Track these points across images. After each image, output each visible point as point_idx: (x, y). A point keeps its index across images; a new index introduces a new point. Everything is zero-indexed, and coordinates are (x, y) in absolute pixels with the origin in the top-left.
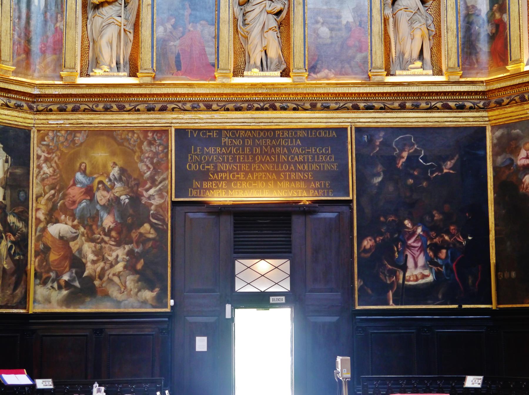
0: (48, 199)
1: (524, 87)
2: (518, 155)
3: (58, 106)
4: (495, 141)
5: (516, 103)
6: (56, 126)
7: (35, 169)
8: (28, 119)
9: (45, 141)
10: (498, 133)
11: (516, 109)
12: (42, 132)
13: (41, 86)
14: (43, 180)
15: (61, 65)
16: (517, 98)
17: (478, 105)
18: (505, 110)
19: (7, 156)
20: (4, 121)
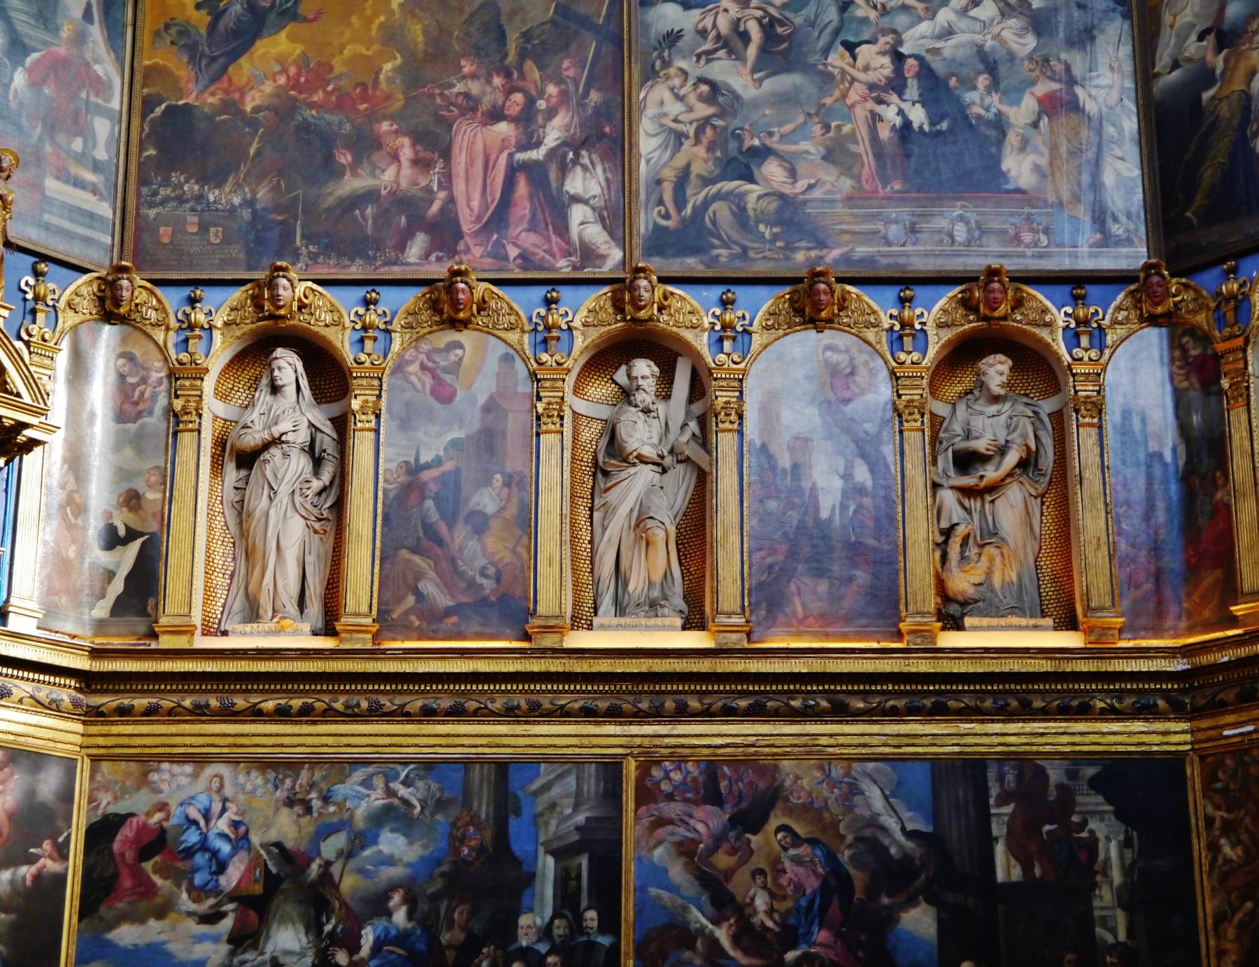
0: (1242, 926)
3: (1237, 690)
6: (1238, 739)
7: (1203, 854)
8: (1176, 733)
9: (1218, 780)
12: (1210, 759)
13: (1187, 651)
14: (1224, 878)
15: (1235, 589)
19: (1126, 832)
20: (1113, 749)
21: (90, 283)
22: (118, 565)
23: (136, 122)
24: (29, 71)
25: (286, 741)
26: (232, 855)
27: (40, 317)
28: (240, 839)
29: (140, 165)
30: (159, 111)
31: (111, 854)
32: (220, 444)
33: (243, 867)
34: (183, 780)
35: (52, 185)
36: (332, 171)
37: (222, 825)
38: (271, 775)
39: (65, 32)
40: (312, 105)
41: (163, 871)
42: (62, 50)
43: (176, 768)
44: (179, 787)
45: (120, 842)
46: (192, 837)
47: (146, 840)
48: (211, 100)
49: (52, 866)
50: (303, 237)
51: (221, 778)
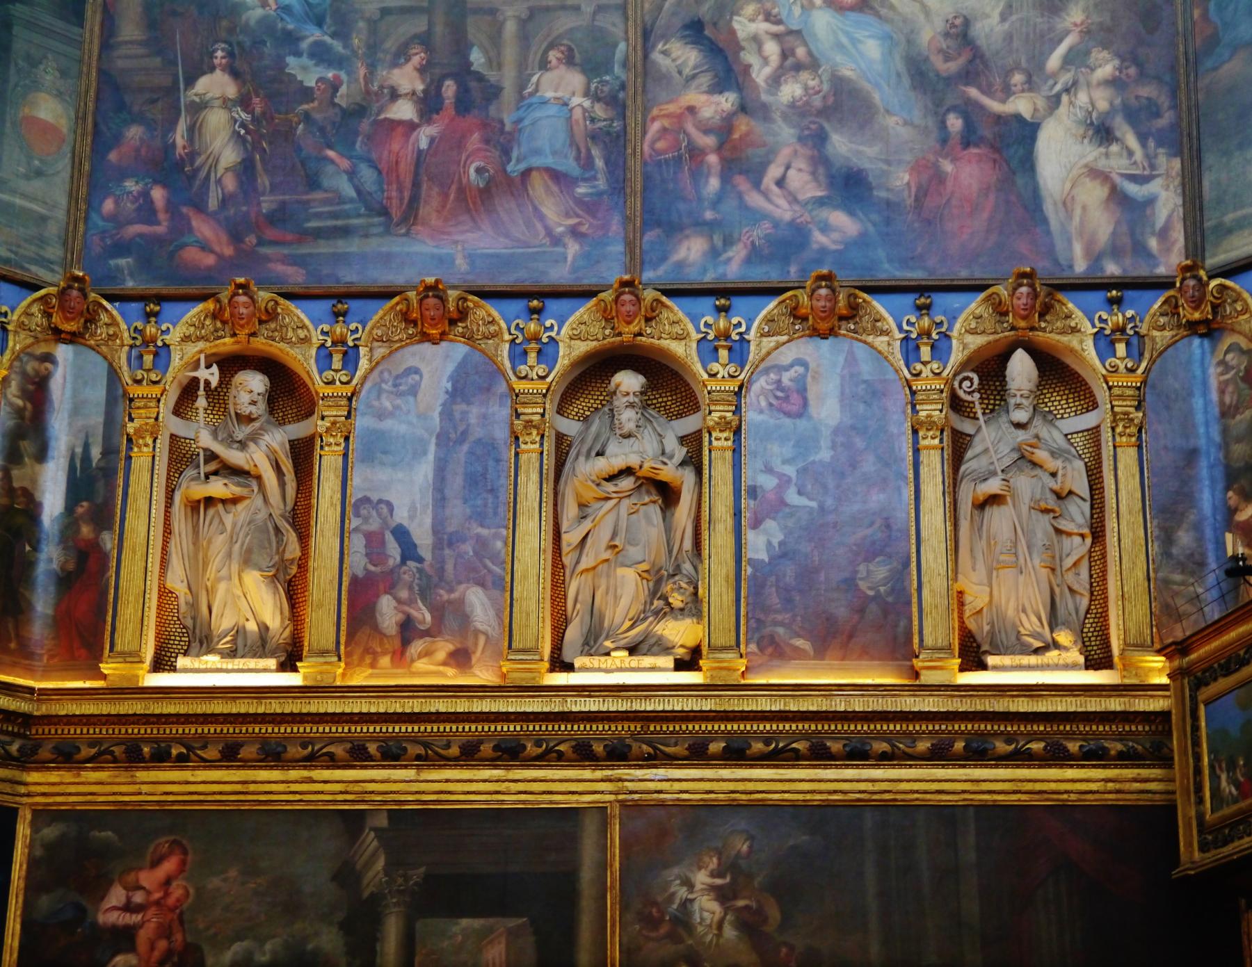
1: (144, 724)
2: (102, 898)
4: (38, 852)
5: (115, 760)
10: (50, 832)
11: (110, 776)
16: (118, 750)
17: (7, 747)
18: (79, 775)
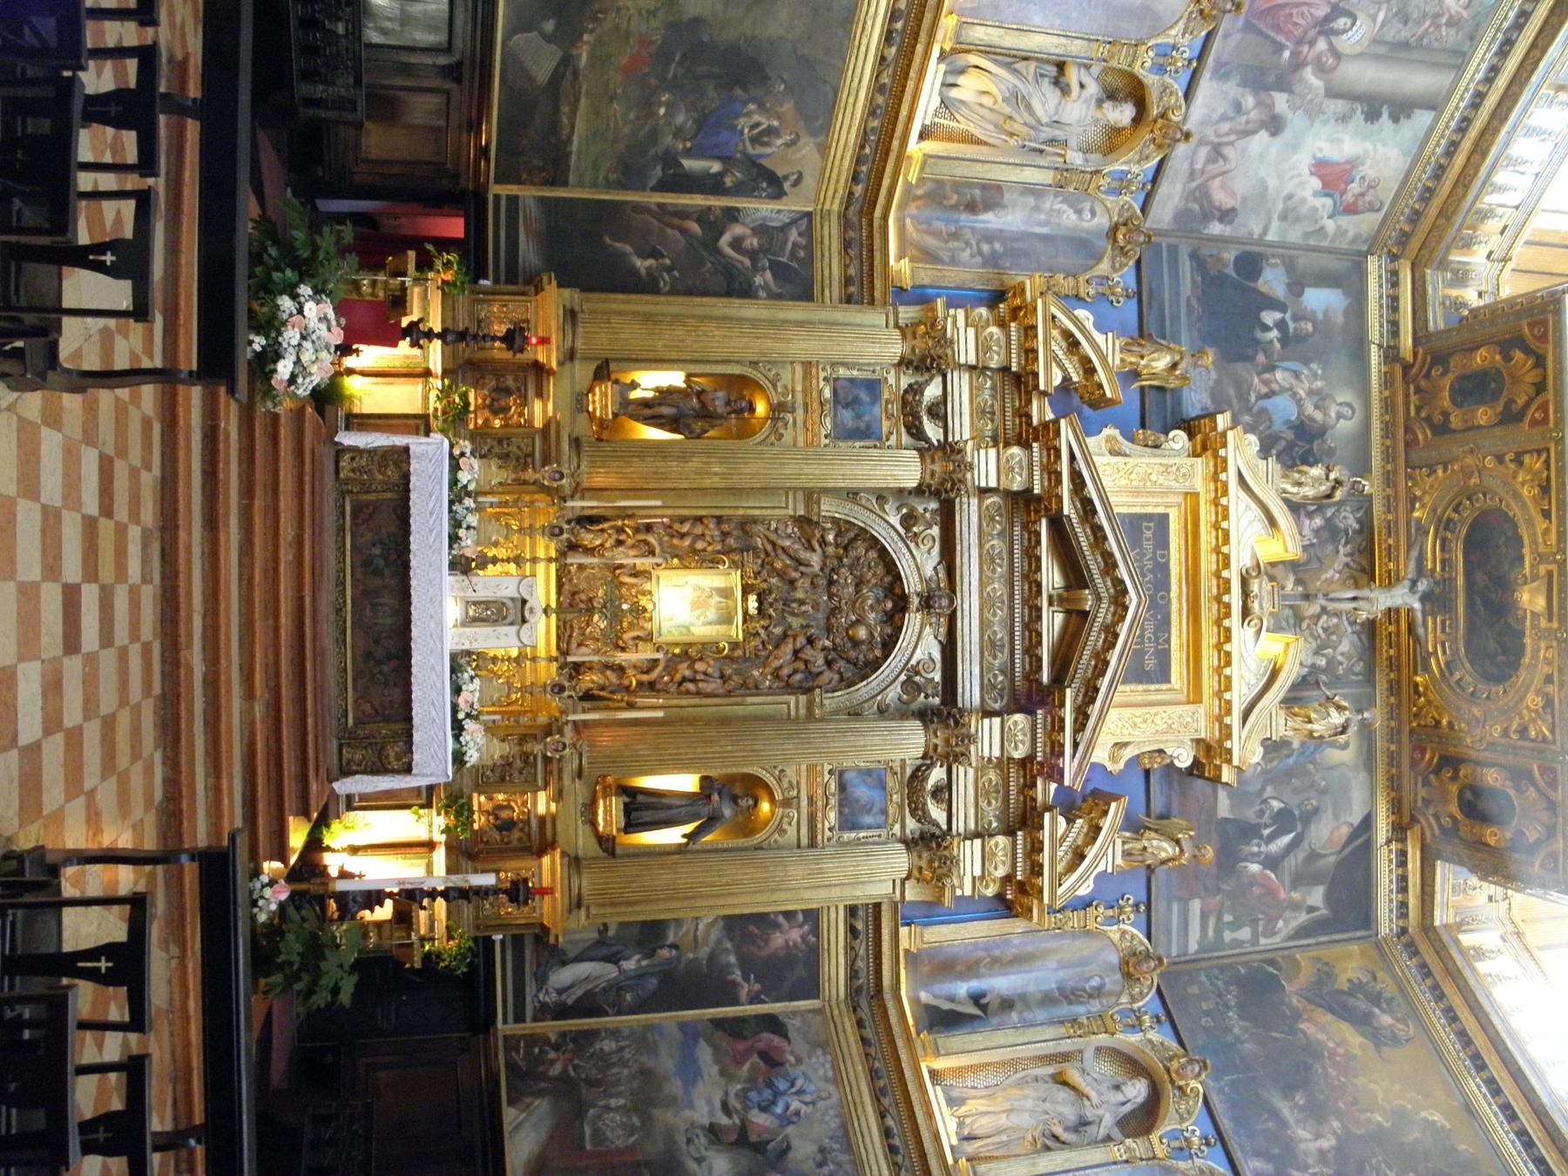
21: (1142, 943)
22: (960, 1003)
23: (1258, 957)
24: (1262, 873)
25: (867, 1139)
26: (774, 1114)
27: (1110, 912)
28: (787, 1119)
29: (1231, 965)
30: (1271, 969)
31: (757, 1033)
32: (1065, 1057)
33: (767, 1124)
34: (821, 1072)
35: (1196, 905)
36: (1288, 1091)
37: (795, 1104)
38: (840, 1133)
39: (1296, 895)
40: (1324, 1068)
41: (754, 1068)
42: (1283, 895)
43: (828, 1066)
44: (816, 1070)
45: (768, 1037)
46: (782, 1085)
47: (773, 1054)
48: (1294, 1001)
49: (744, 993)
50: (1233, 1082)
51: (829, 1097)
